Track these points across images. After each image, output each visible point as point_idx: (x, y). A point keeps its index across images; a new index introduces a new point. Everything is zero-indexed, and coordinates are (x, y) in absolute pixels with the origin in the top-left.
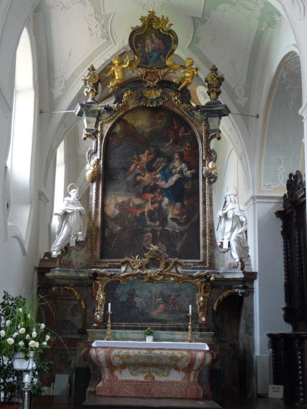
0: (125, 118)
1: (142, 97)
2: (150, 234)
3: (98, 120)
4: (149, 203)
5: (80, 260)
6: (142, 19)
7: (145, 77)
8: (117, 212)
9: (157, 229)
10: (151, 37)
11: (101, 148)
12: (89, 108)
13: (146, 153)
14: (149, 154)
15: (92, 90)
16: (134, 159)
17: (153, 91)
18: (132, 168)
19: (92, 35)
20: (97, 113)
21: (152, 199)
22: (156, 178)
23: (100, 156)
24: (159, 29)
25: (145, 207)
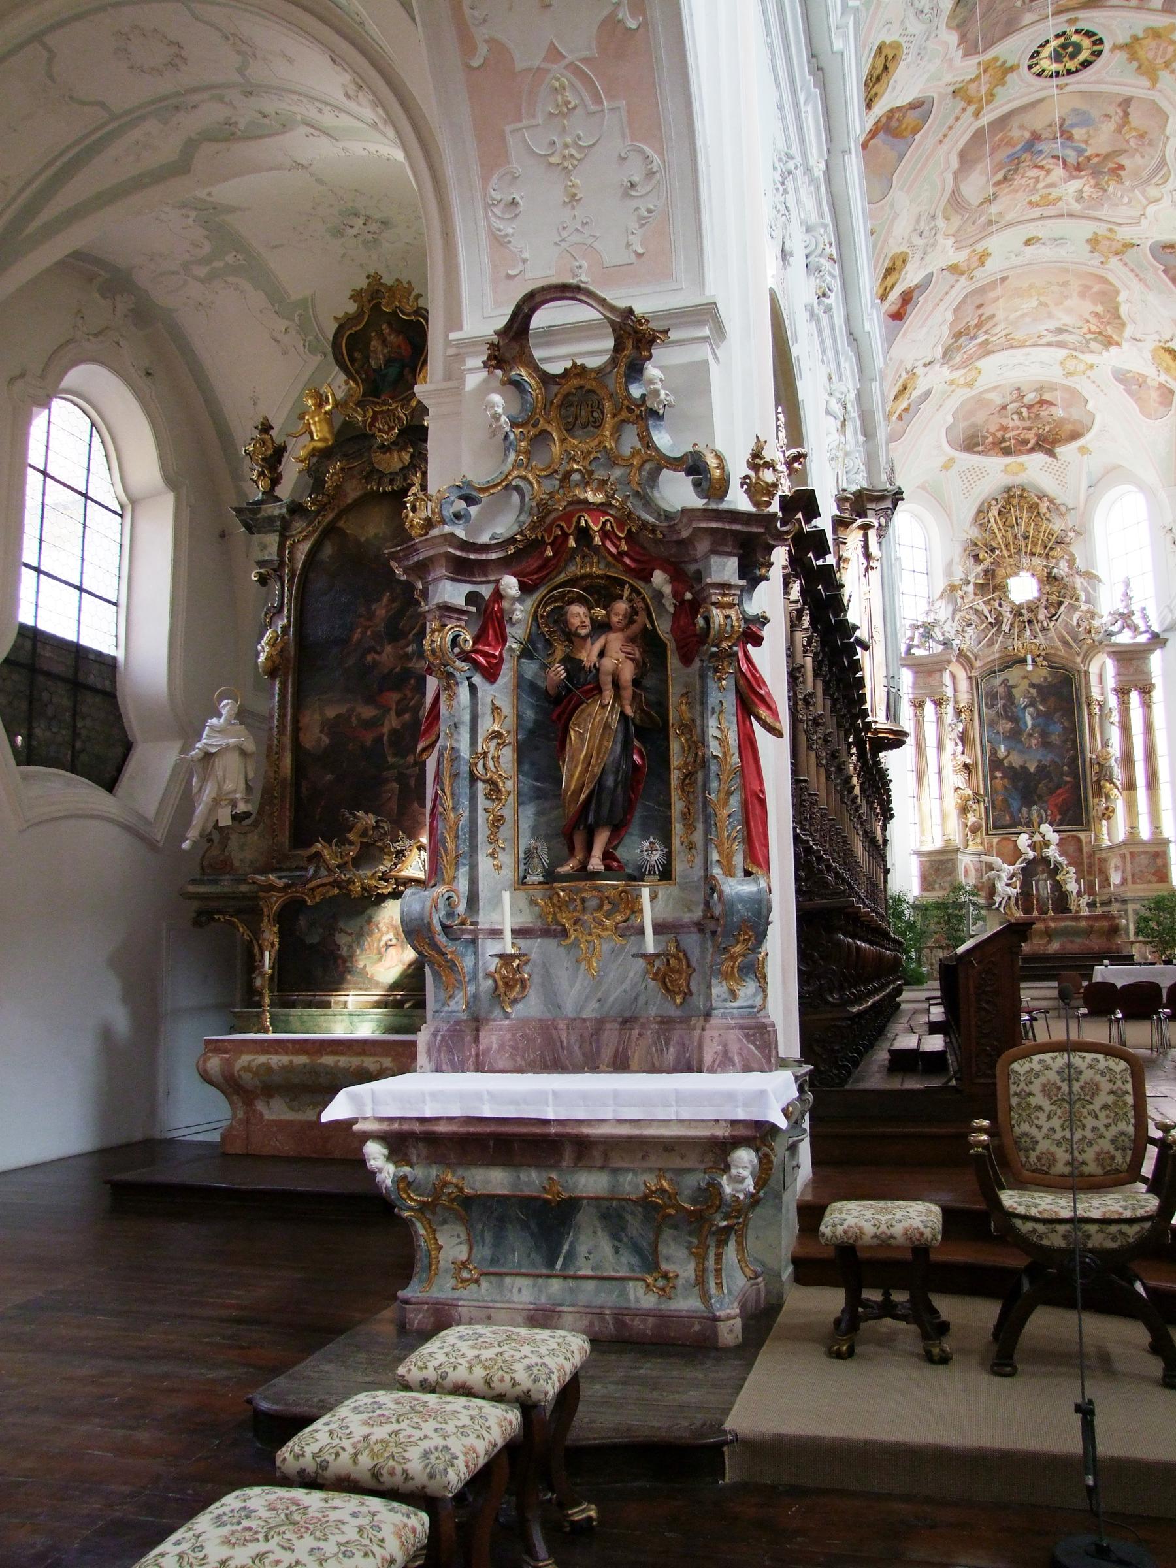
0: (341, 524)
1: (373, 473)
2: (395, 785)
3: (283, 538)
4: (393, 713)
5: (248, 855)
6: (356, 296)
7: (372, 425)
8: (326, 740)
9: (408, 771)
10: (380, 334)
11: (290, 600)
12: (256, 514)
13: (385, 600)
14: (392, 600)
15: (262, 474)
16: (360, 616)
17: (395, 455)
18: (357, 636)
19: (285, 353)
20: (278, 523)
21: (398, 703)
22: (407, 654)
23: (289, 618)
24: (394, 313)
25: (382, 725)
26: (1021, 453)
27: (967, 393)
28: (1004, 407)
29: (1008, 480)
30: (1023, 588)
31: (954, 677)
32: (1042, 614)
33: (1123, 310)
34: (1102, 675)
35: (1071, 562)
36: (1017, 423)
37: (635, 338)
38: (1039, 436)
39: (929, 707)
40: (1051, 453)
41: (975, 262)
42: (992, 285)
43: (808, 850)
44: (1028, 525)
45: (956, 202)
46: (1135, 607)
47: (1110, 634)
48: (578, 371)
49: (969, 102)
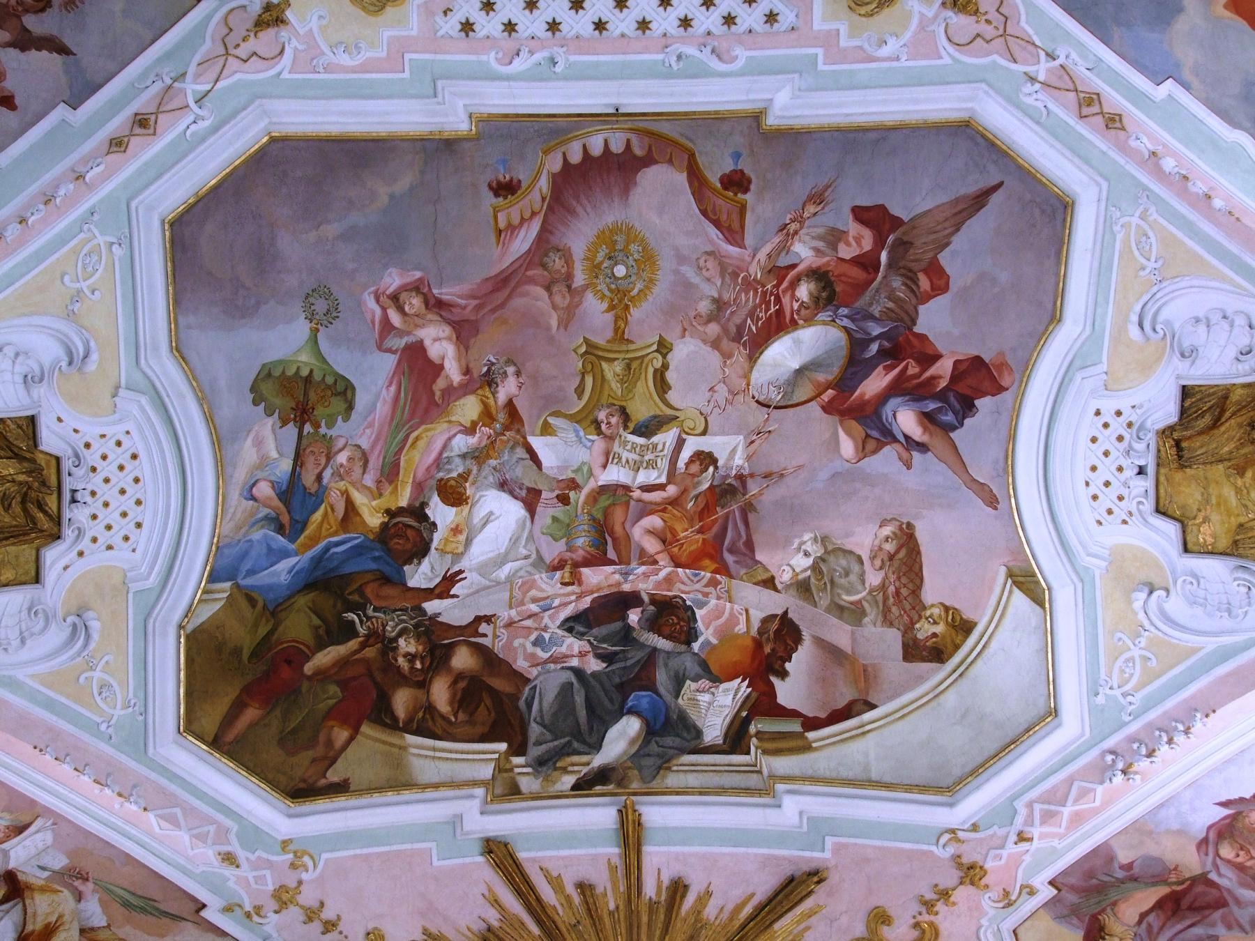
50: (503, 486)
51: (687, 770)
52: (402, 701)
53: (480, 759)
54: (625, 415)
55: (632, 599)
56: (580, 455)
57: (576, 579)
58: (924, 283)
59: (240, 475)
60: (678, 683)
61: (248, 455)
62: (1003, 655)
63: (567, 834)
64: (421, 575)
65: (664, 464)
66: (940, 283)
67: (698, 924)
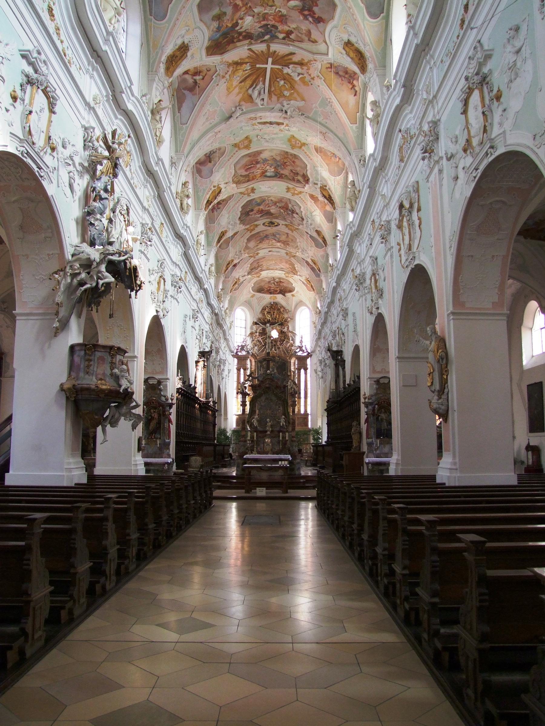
26: (275, 294)
27: (258, 279)
28: (269, 282)
29: (272, 301)
30: (275, 334)
31: (251, 361)
32: (278, 343)
33: (296, 268)
34: (293, 363)
35: (288, 328)
36: (273, 285)
37: (159, 382)
38: (281, 290)
39: (242, 371)
40: (284, 295)
41: (255, 255)
42: (261, 259)
43: (179, 433)
44: (276, 315)
45: (247, 248)
46: (303, 345)
47: (296, 352)
48: (153, 384)
49: (248, 230)
50: (249, 16)
51: (276, 41)
52: (235, 40)
53: (247, 42)
54: (268, 5)
55: (269, 24)
56: (261, 10)
57: (260, 22)
58: (315, 4)
59: (211, 30)
60: (275, 33)
61: (212, 27)
62: (322, 47)
63: (260, 47)
64: (238, 28)
65: (274, 11)
66: (317, 5)
67: (278, 55)
